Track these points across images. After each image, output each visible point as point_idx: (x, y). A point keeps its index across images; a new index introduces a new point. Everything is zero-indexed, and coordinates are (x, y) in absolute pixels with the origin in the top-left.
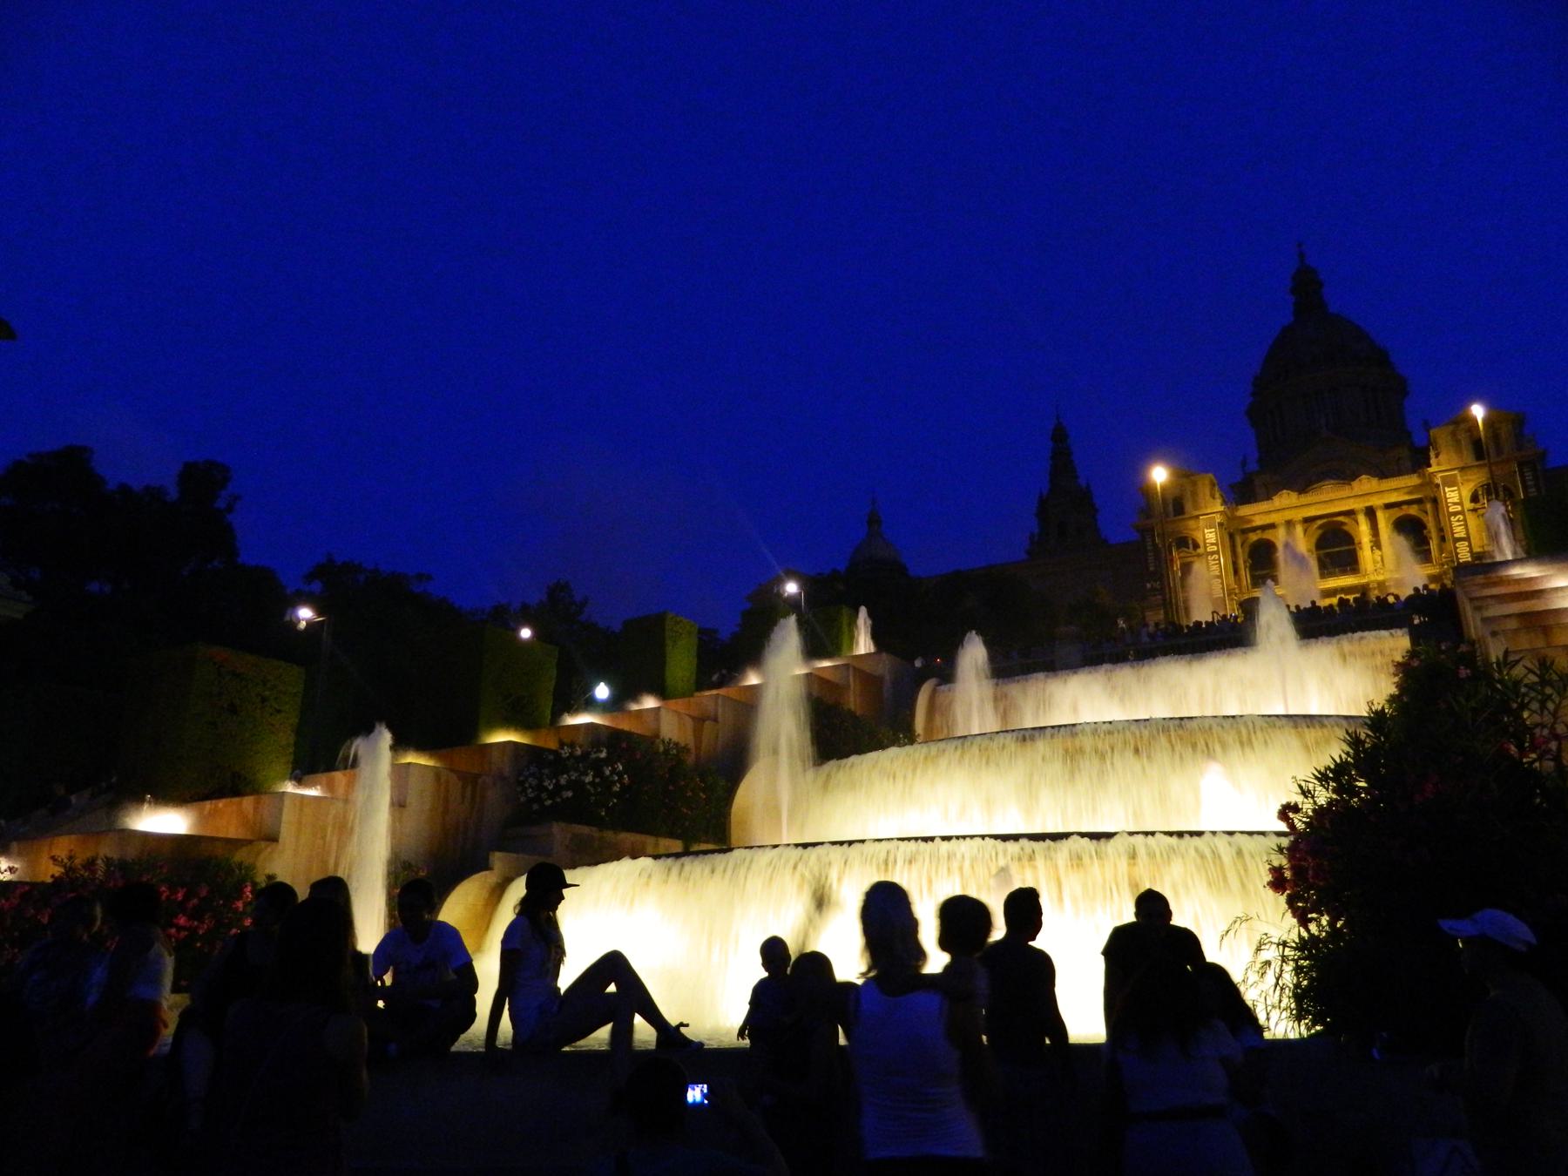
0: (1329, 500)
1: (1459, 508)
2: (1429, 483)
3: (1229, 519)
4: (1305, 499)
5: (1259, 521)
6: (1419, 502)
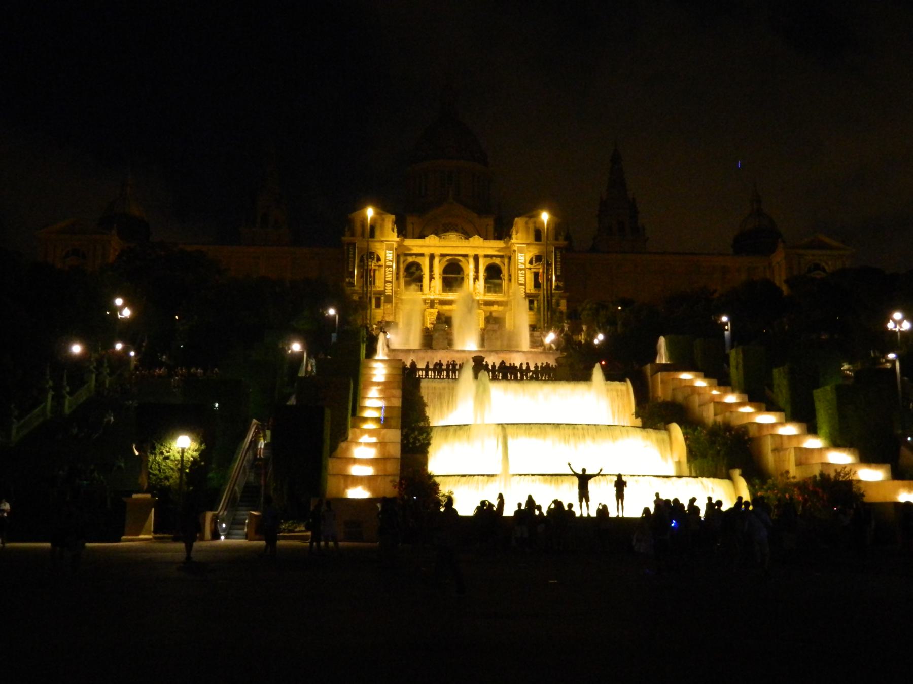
0: (451, 245)
1: (523, 267)
2: (507, 248)
4: (444, 243)
5: (415, 250)
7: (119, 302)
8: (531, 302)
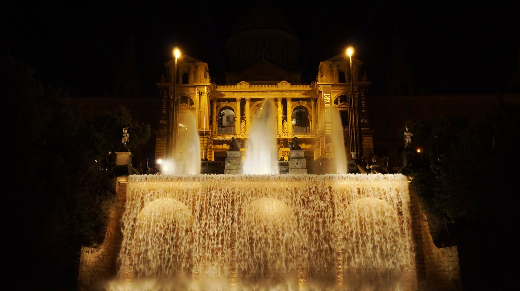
2: (314, 91)
5: (228, 96)
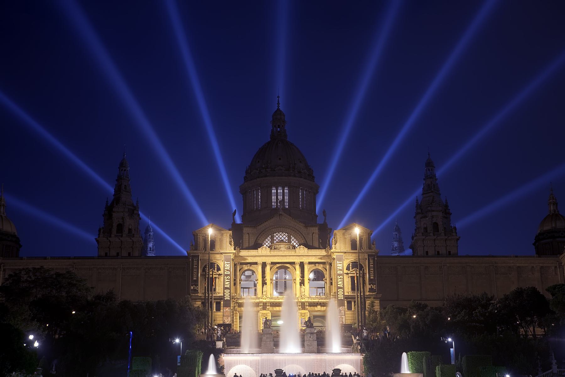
2: (329, 256)
3: (235, 256)
5: (250, 260)
6: (324, 263)
7: (31, 337)
8: (349, 303)
